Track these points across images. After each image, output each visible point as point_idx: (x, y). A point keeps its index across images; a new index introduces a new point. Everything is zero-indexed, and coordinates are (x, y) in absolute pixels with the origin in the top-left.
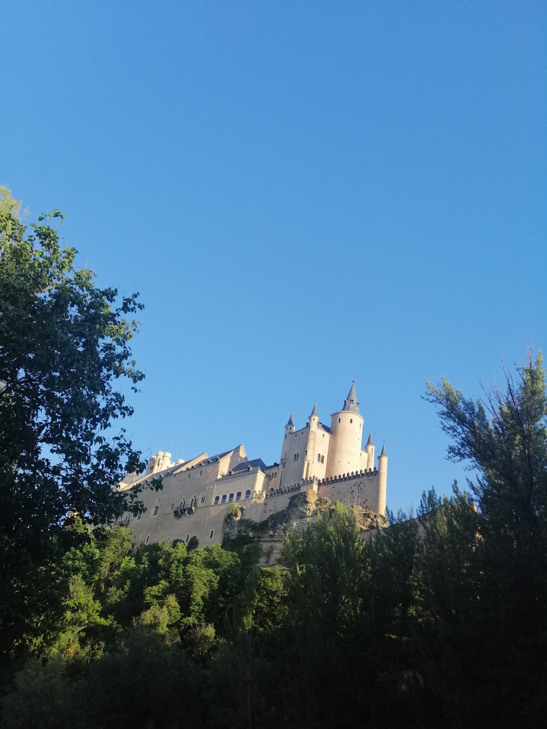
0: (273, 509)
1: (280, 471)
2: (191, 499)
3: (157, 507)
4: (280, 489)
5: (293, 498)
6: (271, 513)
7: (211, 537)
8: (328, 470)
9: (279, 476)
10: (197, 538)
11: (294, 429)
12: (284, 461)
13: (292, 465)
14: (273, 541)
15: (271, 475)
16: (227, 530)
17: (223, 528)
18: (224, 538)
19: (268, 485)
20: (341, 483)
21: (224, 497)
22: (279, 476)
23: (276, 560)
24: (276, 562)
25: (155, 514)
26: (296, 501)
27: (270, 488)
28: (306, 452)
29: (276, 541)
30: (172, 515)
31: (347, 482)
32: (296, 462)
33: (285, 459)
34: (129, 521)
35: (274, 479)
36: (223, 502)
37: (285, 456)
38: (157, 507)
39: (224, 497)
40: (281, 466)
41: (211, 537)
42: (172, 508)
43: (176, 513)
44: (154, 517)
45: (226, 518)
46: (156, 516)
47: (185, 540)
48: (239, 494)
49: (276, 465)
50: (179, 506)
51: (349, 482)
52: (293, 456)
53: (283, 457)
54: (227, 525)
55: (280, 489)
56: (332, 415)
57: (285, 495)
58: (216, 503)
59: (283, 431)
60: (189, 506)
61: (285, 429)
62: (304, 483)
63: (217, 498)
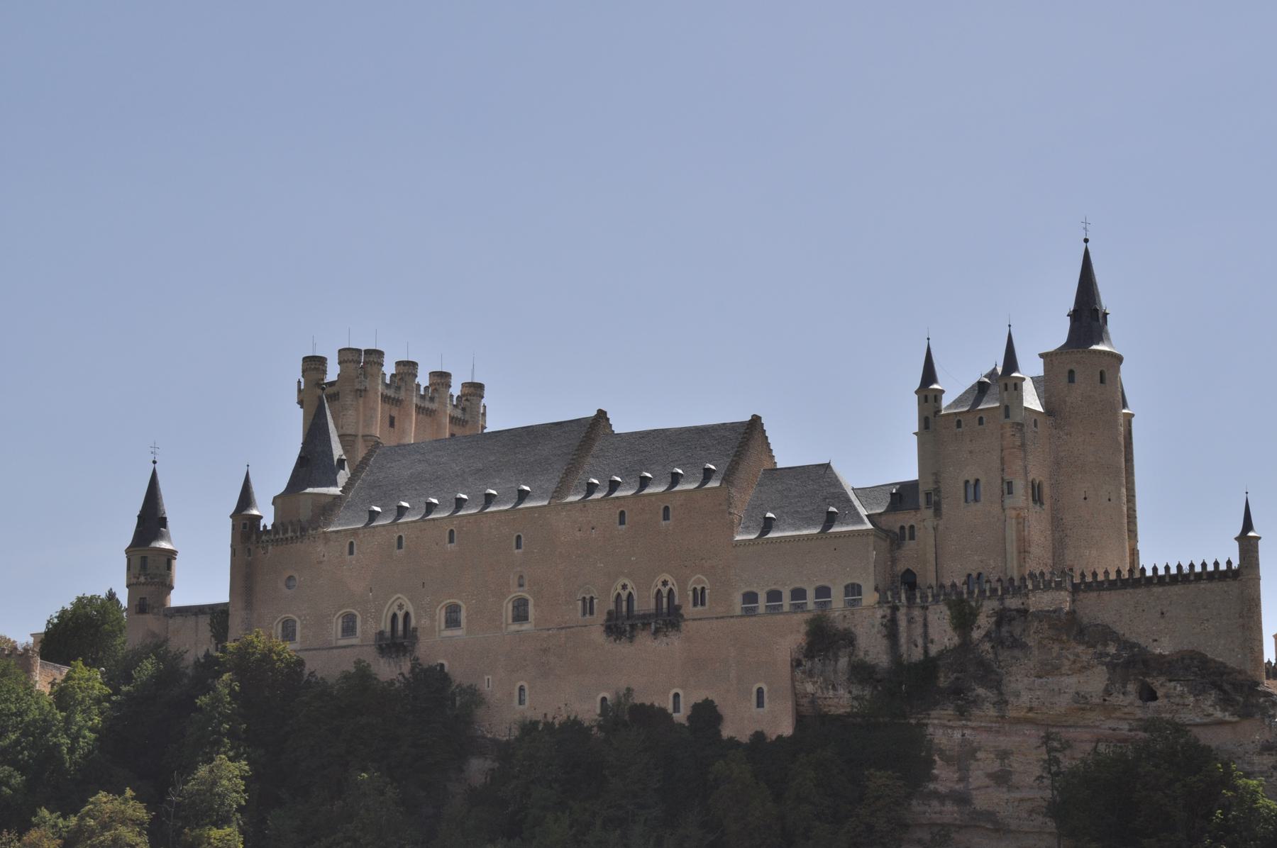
7: (760, 704)
14: (965, 727)
15: (897, 530)
16: (810, 688)
17: (793, 680)
18: (797, 704)
19: (894, 561)
20: (1139, 591)
21: (774, 596)
23: (989, 775)
24: (987, 781)
27: (901, 567)
28: (1010, 484)
29: (973, 728)
30: (597, 634)
35: (909, 545)
36: (774, 610)
37: (937, 482)
39: (774, 596)
41: (760, 704)
44: (515, 627)
46: (526, 627)
47: (670, 708)
48: (823, 592)
50: (612, 607)
51: (1160, 589)
52: (962, 484)
58: (749, 613)
62: (1036, 587)
63: (750, 597)
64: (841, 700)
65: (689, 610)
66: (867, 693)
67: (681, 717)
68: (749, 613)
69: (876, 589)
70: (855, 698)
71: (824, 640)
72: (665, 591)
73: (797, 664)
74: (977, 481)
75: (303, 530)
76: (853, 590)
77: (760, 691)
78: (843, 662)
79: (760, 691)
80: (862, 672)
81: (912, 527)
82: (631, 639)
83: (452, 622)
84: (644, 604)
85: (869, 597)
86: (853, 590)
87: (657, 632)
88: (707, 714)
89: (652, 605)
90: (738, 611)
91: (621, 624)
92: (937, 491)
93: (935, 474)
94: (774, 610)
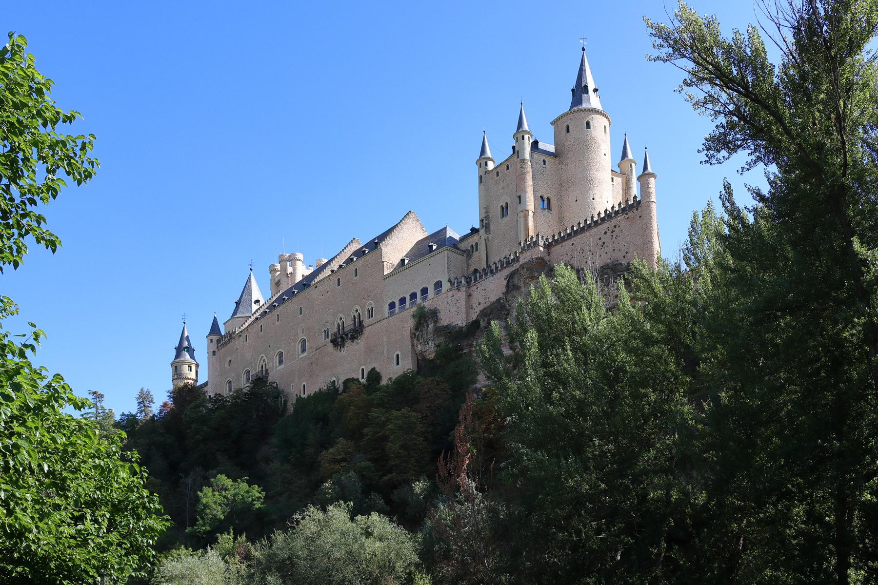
0: (482, 301)
1: (483, 238)
2: (352, 317)
3: (304, 342)
4: (488, 266)
5: (511, 276)
6: (481, 307)
7: (398, 364)
8: (561, 219)
9: (482, 247)
10: (378, 370)
11: (491, 166)
12: (486, 221)
13: (499, 225)
16: (419, 348)
17: (413, 345)
19: (468, 266)
20: (583, 235)
21: (403, 301)
22: (482, 247)
25: (304, 350)
26: (516, 280)
27: (472, 269)
28: (520, 197)
30: (330, 347)
31: (592, 231)
32: (506, 219)
33: (487, 217)
34: (267, 371)
35: (476, 254)
36: (402, 309)
37: (486, 213)
38: (304, 342)
40: (482, 232)
41: (398, 364)
42: (326, 336)
43: (334, 342)
45: (413, 331)
46: (306, 354)
49: (474, 231)
50: (336, 330)
52: (499, 209)
53: (483, 216)
54: (418, 340)
55: (488, 266)
56: (552, 124)
57: (498, 275)
58: (392, 314)
59: (474, 172)
60: (352, 327)
61: (477, 167)
63: (392, 306)
64: (430, 350)
65: (367, 321)
66: (442, 339)
67: (363, 381)
68: (392, 314)
69: (449, 281)
70: (438, 346)
71: (424, 318)
72: (356, 315)
73: (413, 335)
74: (507, 204)
75: (231, 335)
76: (438, 285)
77: (398, 355)
78: (431, 326)
79: (398, 355)
80: (440, 331)
81: (477, 244)
82: (343, 345)
83: (281, 362)
84: (349, 324)
85: (446, 286)
86: (438, 285)
87: (353, 338)
88: (374, 376)
89: (352, 322)
90: (387, 315)
91: (340, 340)
92: (487, 217)
93: (486, 208)
94: (402, 309)
